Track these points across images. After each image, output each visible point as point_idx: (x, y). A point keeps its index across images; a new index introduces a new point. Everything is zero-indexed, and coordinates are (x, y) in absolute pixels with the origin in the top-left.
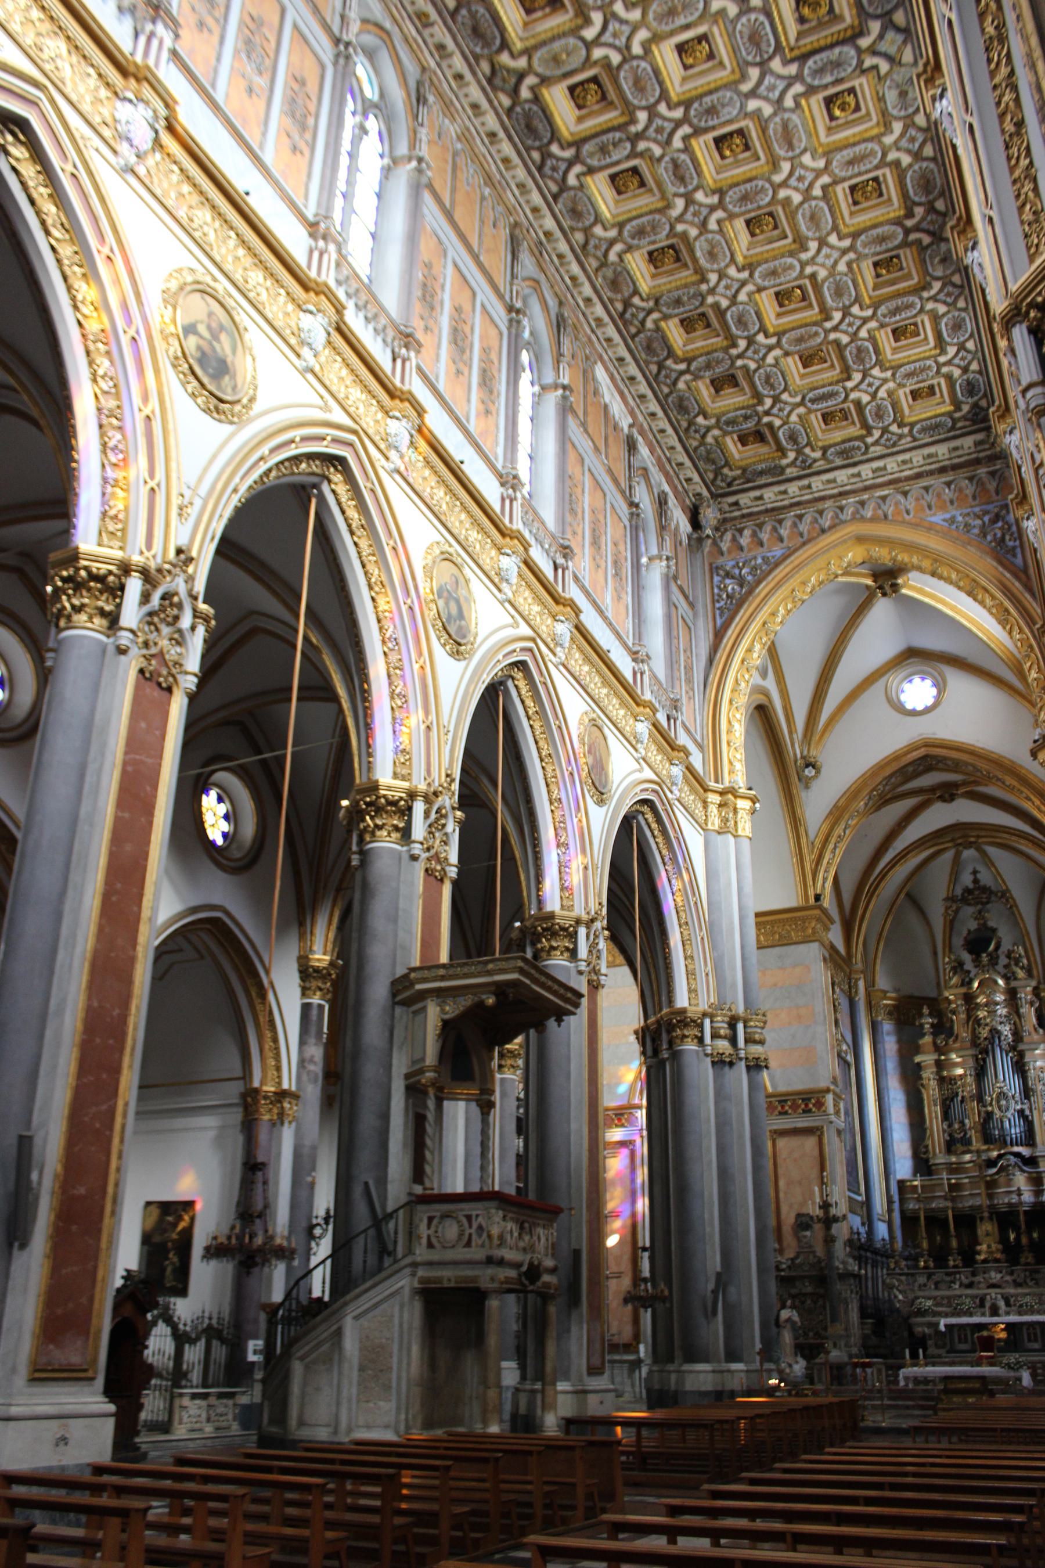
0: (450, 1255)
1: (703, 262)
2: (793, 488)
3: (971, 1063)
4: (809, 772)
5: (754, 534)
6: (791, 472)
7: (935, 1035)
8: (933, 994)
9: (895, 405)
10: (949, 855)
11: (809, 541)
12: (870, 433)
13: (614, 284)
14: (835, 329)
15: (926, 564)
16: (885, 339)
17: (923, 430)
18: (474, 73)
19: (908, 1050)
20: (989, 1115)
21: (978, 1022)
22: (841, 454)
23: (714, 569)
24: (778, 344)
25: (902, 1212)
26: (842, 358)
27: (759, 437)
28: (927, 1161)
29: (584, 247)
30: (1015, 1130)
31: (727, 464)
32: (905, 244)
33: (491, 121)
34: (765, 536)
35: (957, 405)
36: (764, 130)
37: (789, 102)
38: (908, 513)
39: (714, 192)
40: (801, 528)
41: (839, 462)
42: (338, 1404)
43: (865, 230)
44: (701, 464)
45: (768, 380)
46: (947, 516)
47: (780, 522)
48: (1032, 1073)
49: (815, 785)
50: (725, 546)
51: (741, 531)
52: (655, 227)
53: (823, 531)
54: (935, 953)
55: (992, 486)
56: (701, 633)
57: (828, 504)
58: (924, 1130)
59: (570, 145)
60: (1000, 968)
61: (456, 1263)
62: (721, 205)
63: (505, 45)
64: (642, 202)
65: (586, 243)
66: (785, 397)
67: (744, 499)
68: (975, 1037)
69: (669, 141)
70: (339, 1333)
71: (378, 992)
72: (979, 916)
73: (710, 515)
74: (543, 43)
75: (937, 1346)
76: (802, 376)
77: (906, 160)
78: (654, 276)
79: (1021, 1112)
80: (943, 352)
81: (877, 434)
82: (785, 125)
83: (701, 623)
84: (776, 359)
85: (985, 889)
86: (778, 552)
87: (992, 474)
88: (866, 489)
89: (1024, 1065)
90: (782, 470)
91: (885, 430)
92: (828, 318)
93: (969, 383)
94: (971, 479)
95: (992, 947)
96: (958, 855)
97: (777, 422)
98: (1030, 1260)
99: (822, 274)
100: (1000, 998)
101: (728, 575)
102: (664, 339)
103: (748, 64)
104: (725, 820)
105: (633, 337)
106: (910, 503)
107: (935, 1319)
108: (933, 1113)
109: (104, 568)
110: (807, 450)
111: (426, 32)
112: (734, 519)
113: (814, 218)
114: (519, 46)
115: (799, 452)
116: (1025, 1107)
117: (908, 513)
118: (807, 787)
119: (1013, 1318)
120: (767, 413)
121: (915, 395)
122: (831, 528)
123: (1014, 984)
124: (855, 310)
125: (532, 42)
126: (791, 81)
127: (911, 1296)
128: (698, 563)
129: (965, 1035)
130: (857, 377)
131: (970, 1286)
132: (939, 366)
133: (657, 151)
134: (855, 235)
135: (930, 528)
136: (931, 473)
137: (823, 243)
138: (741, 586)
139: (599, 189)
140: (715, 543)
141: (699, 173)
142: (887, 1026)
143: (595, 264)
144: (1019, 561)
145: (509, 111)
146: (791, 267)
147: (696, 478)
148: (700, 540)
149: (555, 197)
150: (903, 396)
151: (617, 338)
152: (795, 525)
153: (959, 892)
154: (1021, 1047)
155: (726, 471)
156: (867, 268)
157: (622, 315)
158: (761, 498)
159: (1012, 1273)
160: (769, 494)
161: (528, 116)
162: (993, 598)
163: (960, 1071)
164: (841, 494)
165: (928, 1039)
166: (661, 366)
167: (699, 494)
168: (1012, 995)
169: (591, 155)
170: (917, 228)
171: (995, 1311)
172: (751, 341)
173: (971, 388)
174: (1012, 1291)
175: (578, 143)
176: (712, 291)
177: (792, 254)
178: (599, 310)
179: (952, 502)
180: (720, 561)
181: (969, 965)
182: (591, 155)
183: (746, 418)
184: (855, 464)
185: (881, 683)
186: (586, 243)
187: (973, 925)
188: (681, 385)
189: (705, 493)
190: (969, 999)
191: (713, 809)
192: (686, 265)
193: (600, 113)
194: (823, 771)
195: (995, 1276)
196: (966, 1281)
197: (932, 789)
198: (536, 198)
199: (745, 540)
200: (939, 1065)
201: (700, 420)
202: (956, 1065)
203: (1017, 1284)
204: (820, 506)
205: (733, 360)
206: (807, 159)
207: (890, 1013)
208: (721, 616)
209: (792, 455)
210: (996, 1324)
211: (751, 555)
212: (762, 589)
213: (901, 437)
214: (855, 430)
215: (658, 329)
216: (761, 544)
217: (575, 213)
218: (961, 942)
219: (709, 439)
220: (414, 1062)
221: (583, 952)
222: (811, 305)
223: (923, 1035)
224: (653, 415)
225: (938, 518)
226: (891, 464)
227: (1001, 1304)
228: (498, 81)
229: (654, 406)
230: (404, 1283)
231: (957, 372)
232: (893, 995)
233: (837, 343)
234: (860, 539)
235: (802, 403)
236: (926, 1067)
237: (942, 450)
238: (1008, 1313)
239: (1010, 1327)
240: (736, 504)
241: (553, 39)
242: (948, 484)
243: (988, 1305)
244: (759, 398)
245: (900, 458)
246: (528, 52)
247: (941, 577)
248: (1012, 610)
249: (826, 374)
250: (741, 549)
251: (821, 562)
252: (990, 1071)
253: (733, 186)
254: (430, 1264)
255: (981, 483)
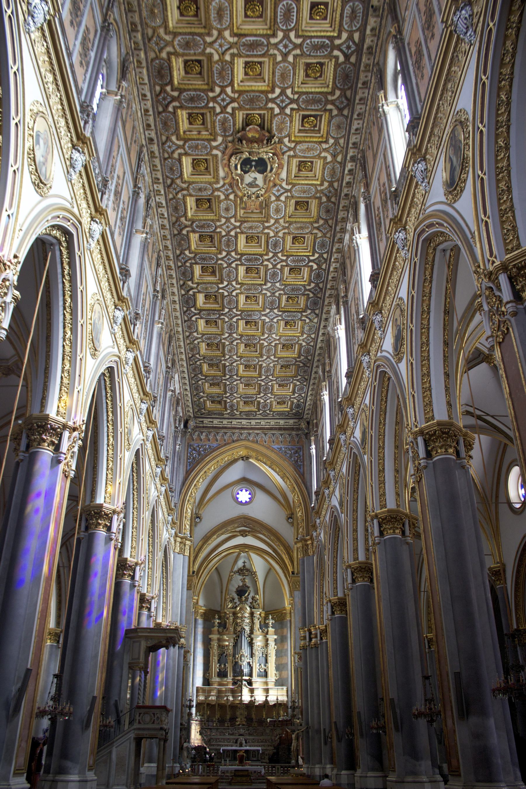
0: (147, 726)
1: (226, 352)
2: (225, 422)
3: (232, 640)
4: (198, 520)
5: (207, 436)
6: (227, 416)
7: (219, 627)
8: (219, 609)
9: (271, 405)
10: (236, 554)
11: (228, 444)
12: (259, 411)
13: (192, 350)
14: (261, 380)
15: (268, 463)
16: (276, 387)
17: (277, 414)
18: (177, 284)
19: (207, 633)
20: (236, 663)
21: (237, 624)
22: (246, 415)
23: (189, 446)
24: (240, 380)
25: (197, 700)
26: (260, 388)
27: (220, 402)
28: (208, 680)
29: (188, 337)
30: (246, 670)
31: (204, 409)
32: (294, 364)
33: (176, 298)
34: (211, 437)
35: (291, 409)
36: (264, 325)
37: (275, 320)
38: (265, 442)
39: (240, 335)
40: (225, 437)
41: (244, 417)
42: (109, 777)
43: (283, 358)
44: (195, 406)
45: (231, 389)
46: (279, 447)
47: (218, 433)
48: (255, 647)
49: (199, 526)
50: (195, 437)
51: (202, 433)
52: (215, 338)
53: (233, 441)
54: (222, 592)
55: (296, 440)
56: (181, 471)
57: (237, 431)
58: (209, 667)
59: (198, 310)
60: (248, 603)
61: (148, 729)
62: (240, 339)
63: (192, 280)
64: (213, 330)
65: (189, 336)
66: (235, 395)
67: (206, 421)
68: (235, 629)
69: (231, 319)
70: (110, 752)
71: (120, 634)
72: (243, 581)
73: (191, 424)
74: (205, 283)
75: (218, 758)
76: (243, 389)
77: (304, 344)
78: (206, 349)
79: (249, 663)
80: (294, 394)
81: (261, 412)
82: (271, 325)
83: (181, 467)
84: (237, 384)
85: (248, 570)
86: (215, 444)
87: (297, 435)
88: (252, 429)
89: (252, 643)
90: (223, 415)
91: (265, 411)
92: (260, 377)
93: (298, 405)
94: (289, 435)
95: (246, 595)
96: (239, 554)
97: (228, 401)
98: (256, 725)
99: (264, 365)
100: (247, 615)
101: (194, 449)
102: (201, 369)
103: (267, 308)
104: (181, 549)
105: (190, 365)
106: (266, 438)
107: (218, 747)
108: (214, 659)
109: (109, 512)
110: (235, 411)
111: (168, 271)
112: (200, 427)
113: (268, 351)
114: (196, 281)
115: (232, 411)
116: (251, 661)
117: (265, 442)
118: (195, 526)
119: (248, 748)
120: (226, 397)
121: (278, 403)
122: (237, 441)
123: (253, 610)
124: (271, 377)
125: (201, 281)
126: (278, 316)
127: (209, 737)
128: (184, 441)
129: (232, 629)
130: (262, 395)
131: (232, 734)
132: (291, 398)
133: (227, 320)
134: (279, 358)
135: (273, 450)
136: (275, 429)
137: (268, 357)
138: (199, 455)
139: (201, 323)
140: (191, 435)
141: (237, 329)
142: (200, 621)
143: (188, 342)
144: (302, 470)
145: (183, 295)
146: (255, 361)
147: (191, 411)
148: (185, 432)
149: (185, 321)
150: (274, 403)
151: (185, 365)
152: (223, 436)
153: (236, 569)
154: (252, 636)
155: (203, 410)
156: (279, 367)
157: (190, 358)
158: (212, 422)
159: (248, 730)
160: (216, 422)
161: (189, 298)
162: (290, 482)
163: (227, 643)
164: (242, 428)
165: (216, 628)
166: (195, 375)
167: (190, 416)
168: (252, 614)
169: (204, 314)
170: (300, 362)
171: (241, 745)
172: (231, 376)
173: (298, 406)
174: (248, 737)
175: (201, 310)
176: (225, 360)
177: (257, 357)
178: (183, 357)
179: (281, 442)
180: (192, 443)
181: (236, 600)
182: (204, 314)
183: (218, 397)
184: (250, 419)
185: (231, 488)
186: (189, 336)
187: (241, 584)
188: (200, 382)
189: (192, 416)
190: (235, 614)
191: (178, 544)
192: (219, 350)
193: (212, 304)
194: (203, 520)
195: (242, 731)
196: (231, 732)
197: (240, 532)
198: (179, 322)
199: (203, 437)
200: (219, 640)
201: (202, 394)
202: (226, 641)
203: (250, 734)
204: (234, 431)
205: (222, 380)
206: (274, 336)
207: (201, 616)
208: (190, 465)
209: (229, 411)
210: (241, 750)
211: (204, 443)
212: (208, 459)
213: (269, 414)
214: (254, 409)
215: (201, 365)
216: (209, 440)
217: (189, 327)
218: (235, 590)
219: (202, 400)
220: (132, 659)
221: (153, 609)
222: (256, 371)
223: (214, 627)
224: (186, 389)
225: (276, 447)
226: (263, 422)
227: (244, 742)
228: (184, 287)
229: (188, 388)
230: (132, 735)
231: (295, 401)
232: (204, 608)
233: (260, 384)
234: (247, 448)
235: (240, 398)
236: (213, 640)
237: (282, 422)
238: (246, 746)
239: (247, 751)
240: (202, 421)
241: (208, 283)
242: (281, 435)
243: (239, 742)
244: (225, 394)
245: (266, 421)
246: (198, 284)
247: (272, 469)
248: (296, 488)
249: (251, 391)
250: (201, 440)
251: (230, 453)
252: (239, 644)
253: (247, 335)
254: (139, 729)
255: (293, 438)
